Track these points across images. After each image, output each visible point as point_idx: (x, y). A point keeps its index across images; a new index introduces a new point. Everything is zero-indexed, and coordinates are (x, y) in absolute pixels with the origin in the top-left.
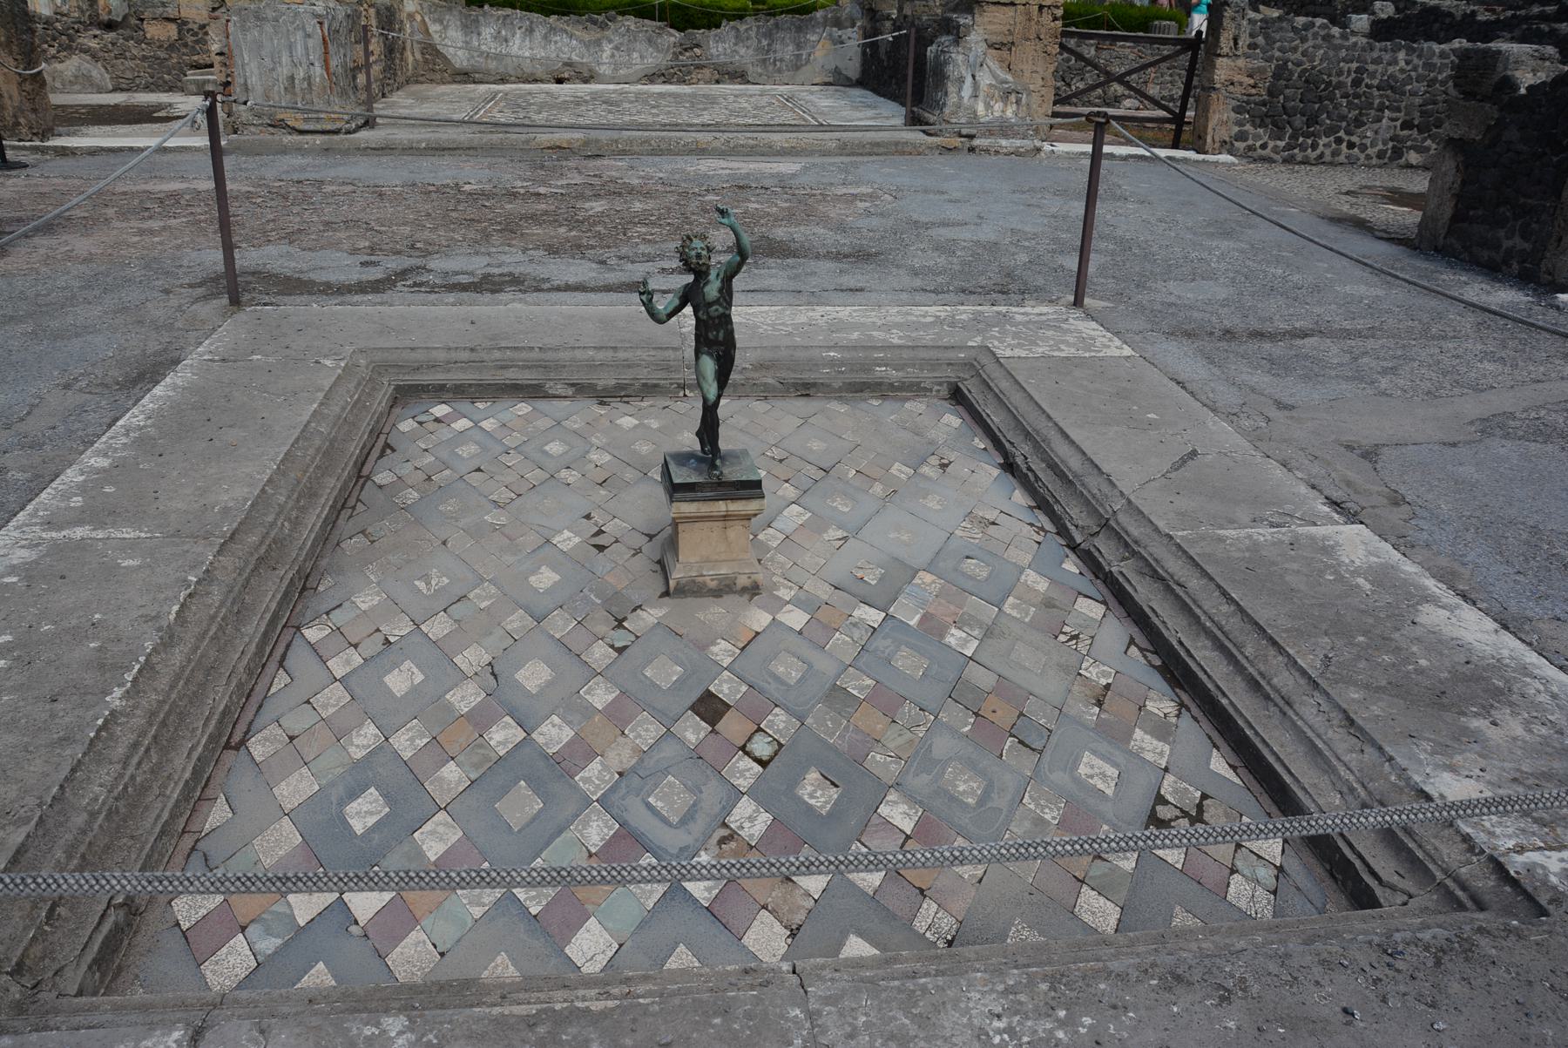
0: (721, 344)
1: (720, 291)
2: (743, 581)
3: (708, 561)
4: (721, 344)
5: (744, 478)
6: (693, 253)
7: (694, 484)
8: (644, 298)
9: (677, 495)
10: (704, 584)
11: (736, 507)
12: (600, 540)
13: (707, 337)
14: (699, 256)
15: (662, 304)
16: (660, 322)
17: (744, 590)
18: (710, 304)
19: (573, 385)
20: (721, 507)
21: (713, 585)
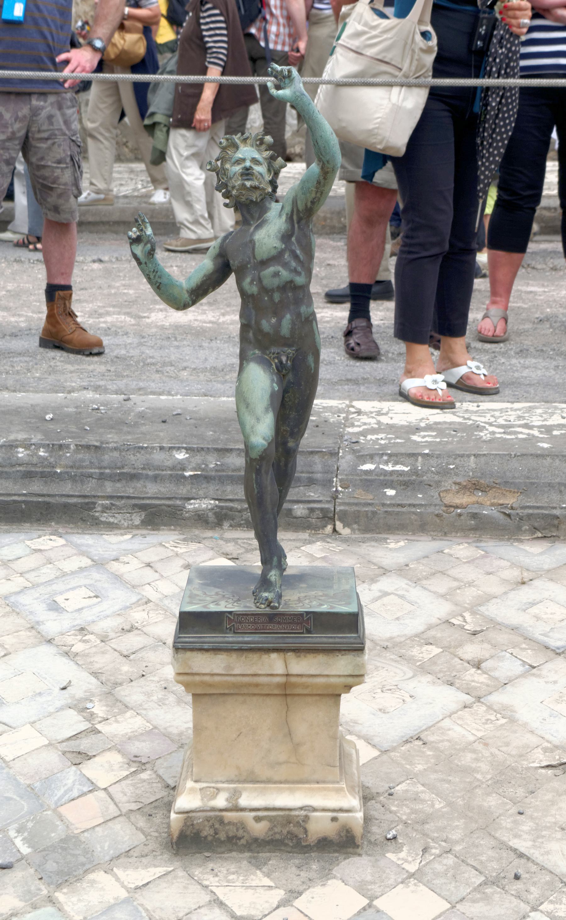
0: (286, 342)
1: (286, 237)
2: (320, 826)
3: (252, 779)
4: (286, 342)
5: (324, 608)
6: (237, 169)
7: (220, 615)
8: (139, 250)
9: (189, 638)
10: (241, 825)
11: (302, 666)
12: (84, 744)
13: (259, 331)
14: (247, 173)
15: (184, 270)
16: (182, 306)
17: (325, 845)
18: (265, 263)
19: (143, 507)
20: (275, 664)
21: (259, 829)
